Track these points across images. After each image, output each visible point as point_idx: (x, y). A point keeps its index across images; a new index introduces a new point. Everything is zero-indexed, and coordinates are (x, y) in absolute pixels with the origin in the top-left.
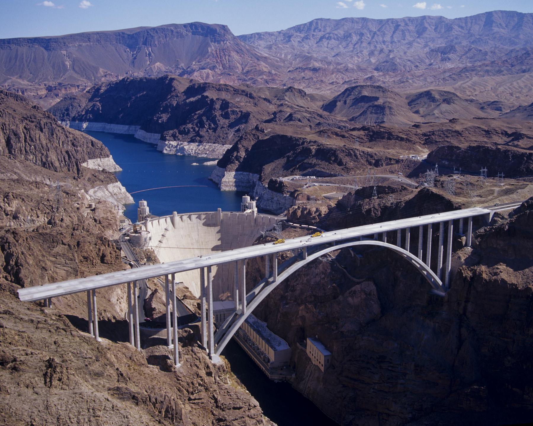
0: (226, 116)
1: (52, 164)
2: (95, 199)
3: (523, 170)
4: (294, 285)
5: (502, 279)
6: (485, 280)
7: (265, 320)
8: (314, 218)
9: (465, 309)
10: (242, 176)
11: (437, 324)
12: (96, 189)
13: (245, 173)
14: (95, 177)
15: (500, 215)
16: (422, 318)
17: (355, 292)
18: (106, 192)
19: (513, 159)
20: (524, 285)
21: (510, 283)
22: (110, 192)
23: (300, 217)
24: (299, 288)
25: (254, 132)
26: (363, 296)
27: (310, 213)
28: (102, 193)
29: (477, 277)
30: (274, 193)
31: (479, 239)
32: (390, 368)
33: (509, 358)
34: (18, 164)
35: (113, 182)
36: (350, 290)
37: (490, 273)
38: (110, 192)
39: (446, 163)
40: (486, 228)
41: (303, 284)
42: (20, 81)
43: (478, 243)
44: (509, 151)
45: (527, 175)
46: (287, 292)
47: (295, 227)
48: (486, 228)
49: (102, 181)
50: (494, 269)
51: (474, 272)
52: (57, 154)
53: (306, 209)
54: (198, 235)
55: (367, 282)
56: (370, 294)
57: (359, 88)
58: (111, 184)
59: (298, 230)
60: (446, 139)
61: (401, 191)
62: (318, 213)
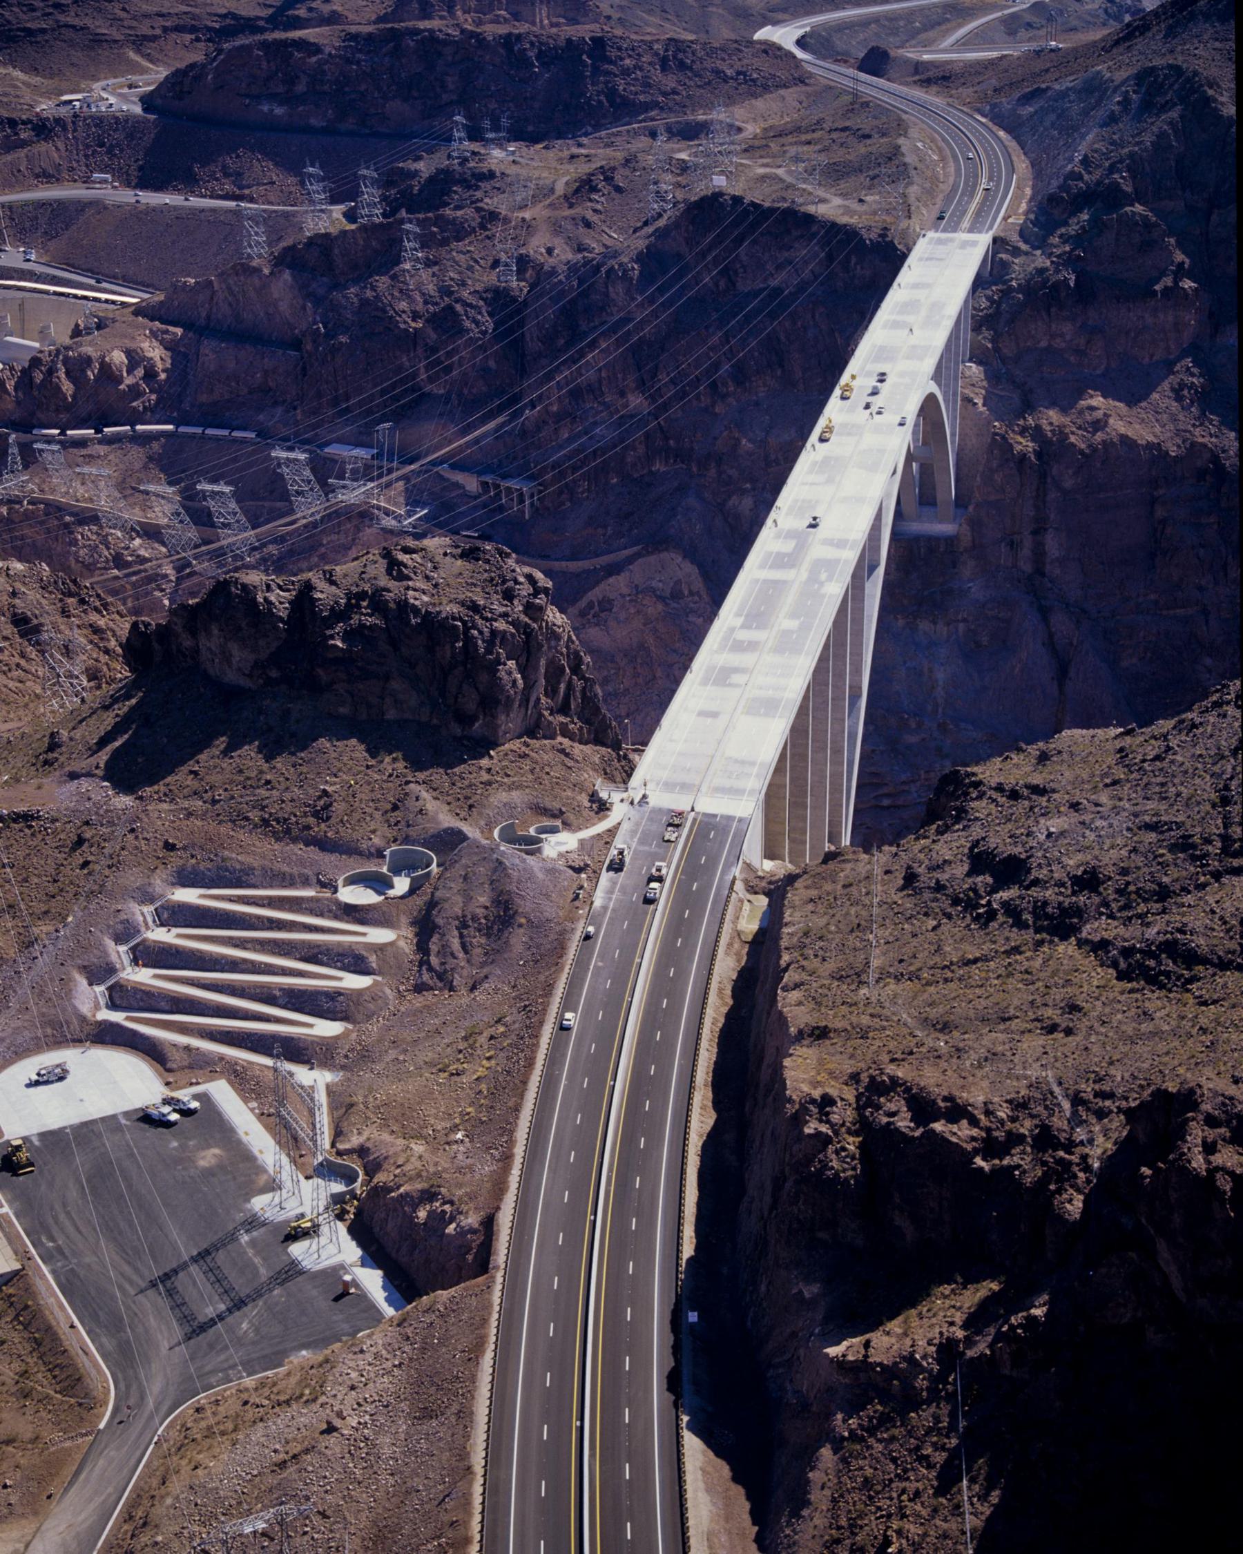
3: (600, 102)
5: (1122, 436)
6: (1082, 452)
8: (135, 392)
9: (1039, 554)
11: (961, 626)
15: (1007, 244)
16: (901, 623)
17: (606, 605)
19: (543, 65)
20: (1180, 442)
21: (1144, 442)
23: (74, 397)
26: (654, 609)
27: (108, 374)
29: (1052, 449)
31: (987, 333)
32: (886, 802)
33: (1208, 661)
36: (583, 603)
37: (1080, 428)
39: (279, 111)
40: (989, 292)
43: (990, 346)
44: (519, 37)
45: (616, 121)
47: (81, 443)
48: (989, 292)
50: (1081, 412)
51: (1037, 434)
53: (88, 361)
55: (652, 559)
56: (676, 595)
59: (102, 450)
60: (62, 18)
61: (483, 227)
62: (140, 372)
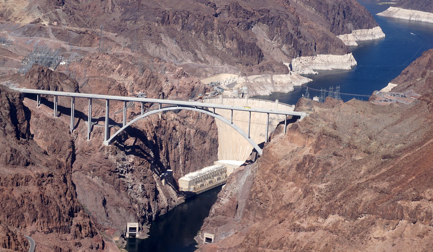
2: (249, 82)
12: (260, 76)
18: (269, 81)
22: (272, 81)
28: (264, 80)
38: (272, 81)
58: (278, 75)
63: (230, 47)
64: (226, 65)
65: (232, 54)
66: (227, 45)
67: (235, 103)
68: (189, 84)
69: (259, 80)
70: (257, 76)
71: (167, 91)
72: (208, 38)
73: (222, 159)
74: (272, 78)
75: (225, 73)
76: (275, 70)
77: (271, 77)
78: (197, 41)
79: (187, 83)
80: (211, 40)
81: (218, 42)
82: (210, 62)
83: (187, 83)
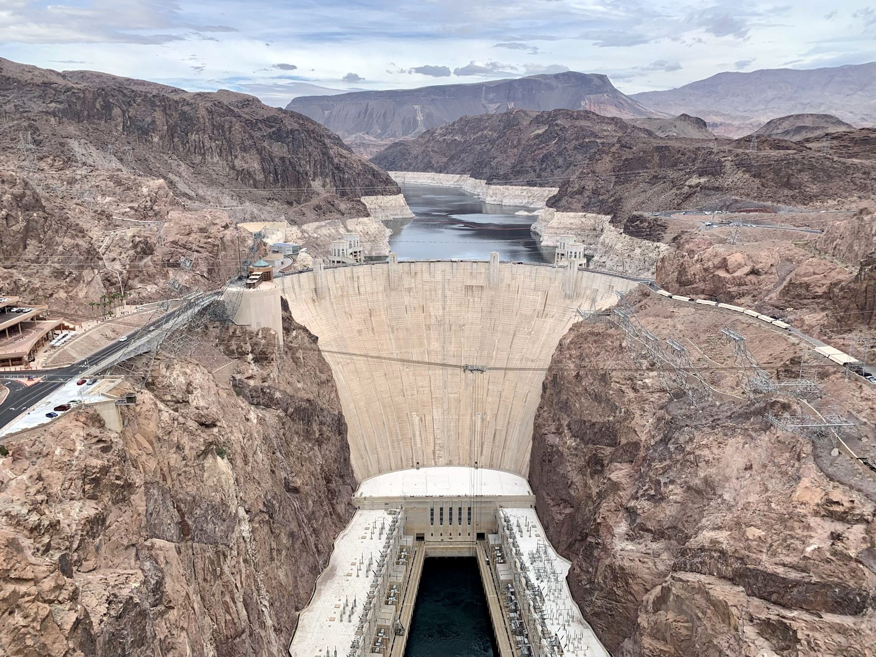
0: (581, 147)
1: (249, 173)
2: (310, 236)
4: (658, 482)
7: (565, 552)
10: (583, 220)
12: (323, 223)
13: (589, 215)
14: (333, 205)
18: (342, 230)
24: (675, 493)
25: (613, 149)
28: (333, 231)
30: (636, 240)
34: (183, 167)
35: (359, 216)
41: (689, 488)
42: (366, 136)
46: (635, 497)
49: (343, 214)
52: (263, 160)
54: (444, 309)
57: (792, 119)
63: (246, 166)
64: (248, 204)
65: (251, 182)
66: (238, 163)
67: (361, 277)
68: (202, 230)
69: (324, 231)
70: (317, 224)
71: (117, 266)
72: (192, 149)
73: (369, 475)
74: (345, 227)
75: (251, 221)
76: (343, 210)
77: (343, 224)
78: (166, 158)
79: (195, 228)
80: (201, 154)
81: (216, 159)
82: (210, 198)
83: (195, 228)
